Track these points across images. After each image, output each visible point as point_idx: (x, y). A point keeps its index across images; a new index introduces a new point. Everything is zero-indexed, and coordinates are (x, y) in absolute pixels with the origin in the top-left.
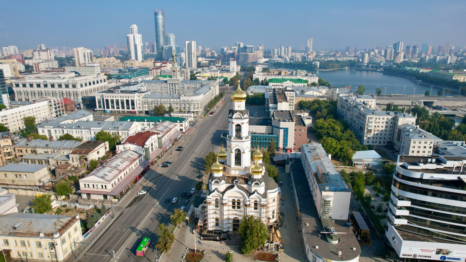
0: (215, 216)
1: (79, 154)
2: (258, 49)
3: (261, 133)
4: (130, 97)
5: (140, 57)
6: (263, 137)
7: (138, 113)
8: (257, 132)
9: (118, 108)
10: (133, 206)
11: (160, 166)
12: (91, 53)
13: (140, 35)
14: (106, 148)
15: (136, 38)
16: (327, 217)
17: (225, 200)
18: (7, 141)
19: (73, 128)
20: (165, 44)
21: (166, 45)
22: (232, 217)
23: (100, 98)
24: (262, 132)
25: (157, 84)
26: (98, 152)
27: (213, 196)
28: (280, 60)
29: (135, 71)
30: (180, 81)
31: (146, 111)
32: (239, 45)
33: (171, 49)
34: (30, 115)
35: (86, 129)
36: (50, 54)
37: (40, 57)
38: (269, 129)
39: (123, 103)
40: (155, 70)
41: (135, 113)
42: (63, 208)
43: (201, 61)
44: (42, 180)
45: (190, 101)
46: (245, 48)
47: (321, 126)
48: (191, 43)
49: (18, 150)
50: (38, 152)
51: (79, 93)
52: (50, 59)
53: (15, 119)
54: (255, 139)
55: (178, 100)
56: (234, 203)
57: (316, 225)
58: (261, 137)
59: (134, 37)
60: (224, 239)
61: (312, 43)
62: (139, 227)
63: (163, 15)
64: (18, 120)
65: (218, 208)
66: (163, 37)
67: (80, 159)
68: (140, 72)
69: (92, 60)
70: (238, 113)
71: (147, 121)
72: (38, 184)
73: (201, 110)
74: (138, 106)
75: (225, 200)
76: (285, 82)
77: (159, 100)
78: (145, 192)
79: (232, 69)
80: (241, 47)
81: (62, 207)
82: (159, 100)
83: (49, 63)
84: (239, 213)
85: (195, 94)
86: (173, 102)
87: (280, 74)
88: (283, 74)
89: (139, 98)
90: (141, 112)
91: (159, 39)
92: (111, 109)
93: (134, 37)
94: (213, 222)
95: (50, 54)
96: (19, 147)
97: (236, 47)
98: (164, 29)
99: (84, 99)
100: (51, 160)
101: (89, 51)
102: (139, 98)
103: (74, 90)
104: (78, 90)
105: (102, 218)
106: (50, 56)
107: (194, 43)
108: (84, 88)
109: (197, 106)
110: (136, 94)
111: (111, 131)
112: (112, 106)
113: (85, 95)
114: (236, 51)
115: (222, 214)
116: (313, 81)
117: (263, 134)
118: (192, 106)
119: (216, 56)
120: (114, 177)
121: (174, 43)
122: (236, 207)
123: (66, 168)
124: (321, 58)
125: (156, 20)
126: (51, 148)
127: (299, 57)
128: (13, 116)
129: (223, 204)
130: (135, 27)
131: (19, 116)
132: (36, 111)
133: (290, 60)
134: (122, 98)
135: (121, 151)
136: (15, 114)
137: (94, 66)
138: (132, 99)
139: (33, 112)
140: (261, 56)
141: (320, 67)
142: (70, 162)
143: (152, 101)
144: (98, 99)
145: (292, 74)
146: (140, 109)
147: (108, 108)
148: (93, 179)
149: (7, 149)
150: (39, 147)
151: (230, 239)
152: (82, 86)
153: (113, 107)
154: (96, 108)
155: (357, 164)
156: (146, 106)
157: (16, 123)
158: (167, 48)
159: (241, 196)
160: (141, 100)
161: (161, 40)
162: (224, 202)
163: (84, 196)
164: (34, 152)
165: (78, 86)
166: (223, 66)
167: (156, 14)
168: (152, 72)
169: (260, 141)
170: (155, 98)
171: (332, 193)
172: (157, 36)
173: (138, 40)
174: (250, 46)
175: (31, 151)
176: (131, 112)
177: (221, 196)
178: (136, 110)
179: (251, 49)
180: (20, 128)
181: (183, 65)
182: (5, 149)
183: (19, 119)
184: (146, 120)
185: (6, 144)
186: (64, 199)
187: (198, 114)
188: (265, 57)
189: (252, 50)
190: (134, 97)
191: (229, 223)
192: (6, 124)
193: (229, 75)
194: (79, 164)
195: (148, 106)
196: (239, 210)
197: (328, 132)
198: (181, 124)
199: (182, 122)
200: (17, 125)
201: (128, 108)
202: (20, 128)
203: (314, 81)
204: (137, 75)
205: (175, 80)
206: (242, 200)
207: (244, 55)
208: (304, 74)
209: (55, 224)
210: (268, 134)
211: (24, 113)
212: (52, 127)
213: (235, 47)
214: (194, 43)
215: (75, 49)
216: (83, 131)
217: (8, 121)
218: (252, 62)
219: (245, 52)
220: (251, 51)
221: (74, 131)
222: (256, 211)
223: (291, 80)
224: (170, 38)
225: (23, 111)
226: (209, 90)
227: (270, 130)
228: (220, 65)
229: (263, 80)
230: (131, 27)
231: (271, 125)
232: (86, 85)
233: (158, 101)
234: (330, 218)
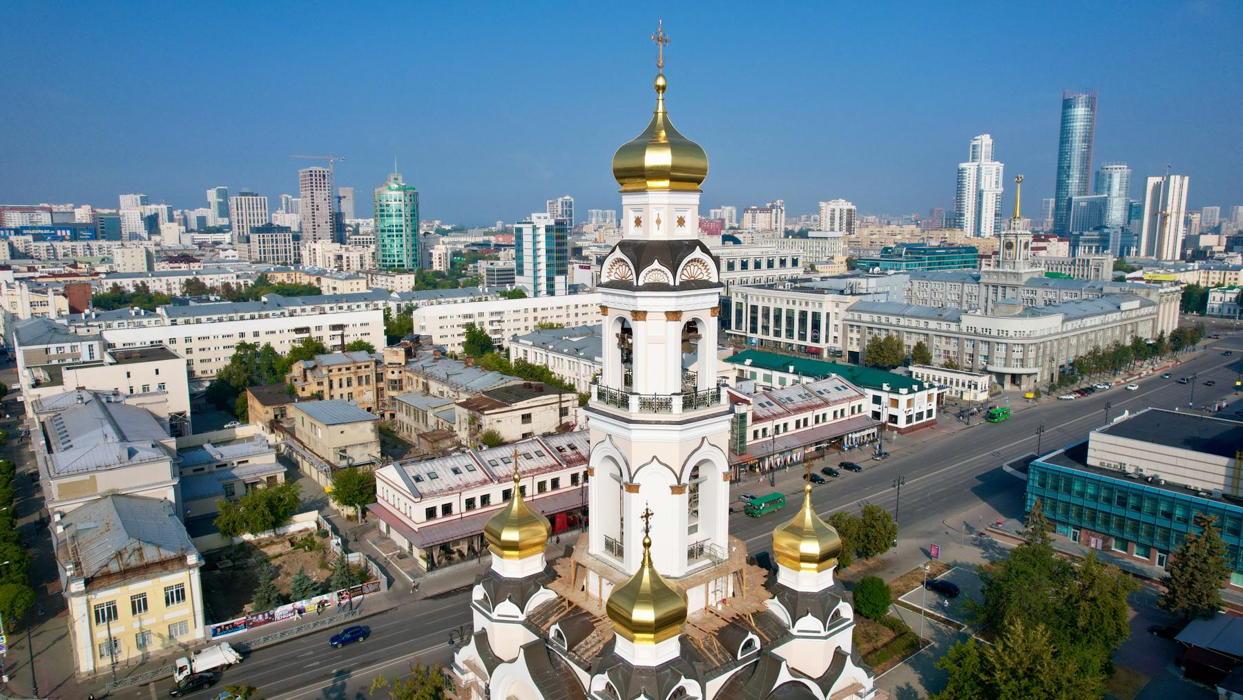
3: (1185, 489)
5: (988, 226)
6: (1188, 506)
8: (1164, 477)
9: (777, 334)
10: (440, 601)
12: (849, 211)
13: (998, 165)
15: (983, 171)
18: (397, 353)
19: (565, 351)
20: (1080, 194)
21: (1084, 195)
24: (1193, 484)
25: (948, 284)
26: (526, 418)
30: (1025, 278)
31: (851, 353)
33: (1099, 208)
37: (755, 225)
39: (790, 320)
41: (818, 352)
43: (1211, 247)
44: (349, 452)
45: (994, 333)
48: (1167, 183)
52: (773, 227)
54: (1138, 509)
55: (953, 327)
58: (1172, 502)
59: (979, 170)
62: (356, 674)
63: (1091, 104)
66: (1082, 172)
68: (943, 258)
71: (795, 372)
73: (1042, 374)
74: (832, 334)
77: (876, 320)
82: (893, 320)
85: (1032, 311)
86: (936, 330)
89: (837, 310)
90: (836, 354)
91: (1068, 176)
92: (760, 335)
93: (979, 170)
98: (1089, 147)
102: (837, 310)
105: (317, 599)
106: (776, 222)
109: (1020, 355)
110: (829, 298)
112: (763, 327)
117: (1196, 492)
118: (1001, 352)
120: (451, 489)
121: (1122, 192)
125: (1065, 120)
128: (516, 316)
130: (985, 142)
131: (531, 320)
132: (577, 315)
134: (791, 306)
136: (522, 312)
137: (826, 238)
139: (568, 315)
142: (456, 428)
143: (873, 322)
147: (754, 330)
154: (730, 328)
156: (855, 335)
158: (1083, 204)
160: (843, 314)
161: (1074, 181)
167: (1067, 105)
169: (1165, 523)
172: (1063, 171)
173: (988, 177)
176: (809, 351)
178: (822, 344)
182: (390, 370)
184: (791, 368)
185: (395, 359)
187: (1019, 385)
190: (820, 305)
192: (496, 332)
198: (895, 396)
199: (898, 393)
201: (803, 337)
204: (930, 264)
205: (1005, 273)
209: (119, 555)
211: (544, 314)
212: (531, 343)
216: (582, 362)
217: (504, 326)
221: (566, 358)
224: (1110, 176)
225: (543, 309)
226: (1110, 312)
230: (975, 143)
233: (891, 325)
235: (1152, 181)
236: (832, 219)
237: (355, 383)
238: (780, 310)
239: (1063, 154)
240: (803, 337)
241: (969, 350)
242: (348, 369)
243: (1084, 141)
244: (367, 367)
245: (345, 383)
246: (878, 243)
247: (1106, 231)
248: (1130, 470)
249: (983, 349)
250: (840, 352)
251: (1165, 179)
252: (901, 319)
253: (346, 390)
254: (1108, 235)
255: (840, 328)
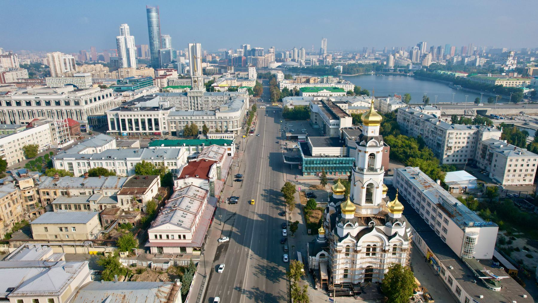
0: (344, 266)
1: (130, 194)
2: (269, 52)
3: (334, 156)
4: (153, 115)
7: (163, 134)
8: (330, 155)
9: (138, 129)
11: (227, 203)
12: (73, 60)
13: (133, 37)
14: (158, 185)
15: (128, 40)
16: (469, 257)
17: (360, 246)
18: (28, 182)
22: (365, 266)
23: (113, 117)
25: (175, 97)
27: (345, 243)
28: (295, 64)
29: (137, 82)
32: (246, 47)
34: (31, 143)
35: (120, 159)
36: (14, 60)
38: (344, 151)
39: (143, 123)
40: (159, 80)
41: (159, 134)
42: (132, 268)
43: (206, 67)
45: (228, 118)
46: (253, 50)
47: (394, 144)
48: (196, 46)
49: (44, 193)
50: (71, 194)
51: (84, 111)
52: (14, 67)
53: (13, 149)
54: (329, 164)
55: (213, 117)
56: (368, 249)
57: (460, 267)
59: (125, 39)
60: (358, 294)
61: (326, 44)
62: (245, 286)
63: (157, 12)
64: (16, 151)
65: (349, 257)
67: (132, 201)
68: (144, 83)
69: (74, 68)
70: (373, 140)
72: (90, 238)
75: (360, 246)
76: (321, 91)
78: (228, 239)
79: (251, 76)
80: (248, 49)
81: (130, 267)
83: (17, 72)
84: (374, 261)
86: (207, 119)
87: (308, 81)
88: (312, 81)
90: (167, 133)
92: (128, 131)
93: (125, 39)
94: (341, 274)
95: (14, 60)
96: (45, 188)
97: (242, 50)
98: (159, 29)
99: (90, 119)
100: (92, 204)
101: (71, 57)
102: (164, 116)
103: (78, 108)
104: (82, 108)
107: (199, 46)
108: (90, 106)
109: (236, 124)
110: (161, 112)
111: (154, 161)
112: (129, 127)
113: (91, 114)
114: (243, 55)
115: (353, 262)
116: (348, 89)
117: (338, 157)
119: (218, 60)
121: (170, 46)
122: (371, 254)
123: (116, 213)
124: (340, 61)
125: (149, 18)
126: (89, 188)
127: (315, 60)
128: (10, 145)
129: (356, 251)
131: (17, 145)
133: (306, 64)
134: (143, 117)
135: (180, 187)
136: (12, 142)
138: (156, 117)
140: (273, 60)
141: (344, 72)
142: (119, 205)
143: (181, 119)
144: (111, 119)
145: (322, 82)
146: (165, 130)
147: (125, 129)
148: (168, 228)
149: (29, 192)
150: (73, 188)
151: (365, 293)
152: (86, 103)
153: (131, 128)
154: (108, 129)
155: (453, 188)
156: (173, 125)
157: (15, 154)
158: (164, 52)
159: (378, 240)
161: (156, 43)
162: (358, 249)
163: (155, 250)
164: (66, 194)
165: (83, 103)
166: (236, 73)
167: (149, 11)
168: (156, 82)
170: (185, 116)
171: (477, 230)
172: (151, 38)
173: (130, 42)
174: (259, 48)
175: (62, 193)
176: (154, 134)
177: (355, 241)
179: (260, 52)
180: (19, 160)
181: (186, 72)
182: (27, 192)
183: (18, 149)
184: (185, 144)
185: (27, 185)
186: (128, 256)
188: (277, 61)
189: (261, 53)
190: (158, 115)
191: (362, 274)
193: (249, 84)
194: (130, 208)
195: (175, 125)
196: (374, 256)
197: (404, 151)
198: (229, 147)
199: (230, 145)
200: (15, 156)
201: (151, 129)
202: (19, 160)
203: (350, 89)
204: (140, 86)
205: (197, 92)
206: (379, 245)
207: (253, 59)
208: (336, 81)
210: (344, 156)
212: (74, 159)
213: (240, 50)
214: (199, 46)
215: (49, 55)
218: (263, 67)
219: (254, 55)
220: (260, 54)
222: (394, 256)
223: (327, 89)
224: (165, 40)
225: (22, 139)
227: (345, 152)
228: (233, 71)
229: (292, 89)
230: (122, 27)
231: (346, 146)
232: (91, 101)
233: (189, 119)
234: (474, 257)
235: (191, 45)
236: (65, 63)
237: (12, 204)
238: (138, 120)
239: (150, 32)
240: (151, 129)
241: (220, 125)
242: (7, 198)
243: (158, 27)
244: (15, 194)
245: (7, 206)
246: (96, 75)
247: (176, 63)
248: (322, 155)
249: (225, 124)
250: (168, 132)
251: (194, 44)
252: (193, 117)
253: (9, 209)
254: (177, 65)
255: (166, 123)
